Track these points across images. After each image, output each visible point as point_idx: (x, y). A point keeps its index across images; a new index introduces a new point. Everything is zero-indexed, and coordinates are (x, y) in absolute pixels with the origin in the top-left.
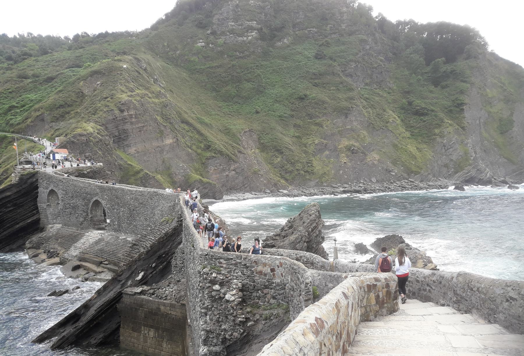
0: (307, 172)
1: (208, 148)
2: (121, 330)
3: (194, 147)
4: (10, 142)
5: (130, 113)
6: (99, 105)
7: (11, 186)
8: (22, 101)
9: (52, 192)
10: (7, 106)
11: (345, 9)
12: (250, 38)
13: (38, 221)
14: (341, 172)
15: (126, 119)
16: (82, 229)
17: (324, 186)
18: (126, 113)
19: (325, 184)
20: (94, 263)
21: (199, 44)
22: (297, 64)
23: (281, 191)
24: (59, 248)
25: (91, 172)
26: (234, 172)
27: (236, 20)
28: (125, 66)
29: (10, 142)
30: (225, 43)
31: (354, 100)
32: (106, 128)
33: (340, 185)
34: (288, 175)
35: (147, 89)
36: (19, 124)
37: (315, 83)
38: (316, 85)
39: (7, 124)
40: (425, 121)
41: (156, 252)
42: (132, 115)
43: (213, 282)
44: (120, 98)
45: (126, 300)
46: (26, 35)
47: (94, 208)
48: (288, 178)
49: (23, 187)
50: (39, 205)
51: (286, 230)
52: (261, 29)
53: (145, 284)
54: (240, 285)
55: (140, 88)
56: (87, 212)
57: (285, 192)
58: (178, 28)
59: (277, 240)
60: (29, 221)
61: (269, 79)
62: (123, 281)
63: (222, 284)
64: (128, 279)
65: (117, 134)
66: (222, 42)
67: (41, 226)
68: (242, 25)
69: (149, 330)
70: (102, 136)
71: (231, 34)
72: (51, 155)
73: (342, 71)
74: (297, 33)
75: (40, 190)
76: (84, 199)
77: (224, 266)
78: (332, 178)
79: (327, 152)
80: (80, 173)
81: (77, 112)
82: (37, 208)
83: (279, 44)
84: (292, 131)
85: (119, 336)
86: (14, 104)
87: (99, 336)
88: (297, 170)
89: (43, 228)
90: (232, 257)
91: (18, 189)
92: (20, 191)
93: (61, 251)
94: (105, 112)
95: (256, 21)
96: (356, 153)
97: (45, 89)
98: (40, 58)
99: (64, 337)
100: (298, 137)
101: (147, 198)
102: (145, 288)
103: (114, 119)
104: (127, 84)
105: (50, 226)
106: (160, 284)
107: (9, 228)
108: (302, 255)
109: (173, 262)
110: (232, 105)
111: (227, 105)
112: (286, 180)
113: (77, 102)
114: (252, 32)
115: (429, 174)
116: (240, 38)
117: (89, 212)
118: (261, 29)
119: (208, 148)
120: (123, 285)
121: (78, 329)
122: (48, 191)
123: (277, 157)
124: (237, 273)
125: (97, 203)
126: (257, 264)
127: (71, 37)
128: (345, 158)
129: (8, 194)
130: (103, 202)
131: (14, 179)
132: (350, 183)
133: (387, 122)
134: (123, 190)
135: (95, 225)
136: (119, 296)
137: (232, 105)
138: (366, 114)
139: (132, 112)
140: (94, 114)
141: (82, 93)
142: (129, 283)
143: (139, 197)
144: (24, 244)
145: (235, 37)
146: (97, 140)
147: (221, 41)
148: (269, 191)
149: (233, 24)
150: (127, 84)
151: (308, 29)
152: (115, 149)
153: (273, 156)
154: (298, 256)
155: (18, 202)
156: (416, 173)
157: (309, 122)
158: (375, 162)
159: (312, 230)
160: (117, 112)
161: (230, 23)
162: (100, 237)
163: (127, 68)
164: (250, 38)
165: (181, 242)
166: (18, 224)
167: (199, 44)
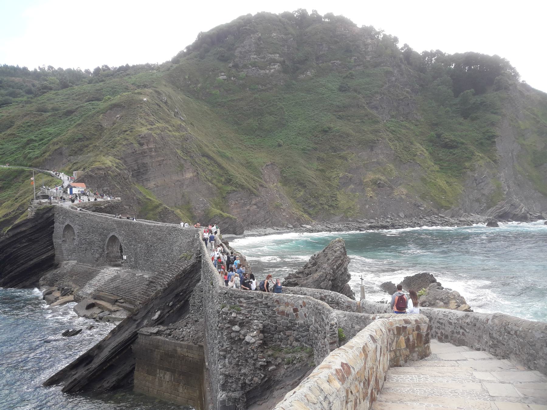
0: (331, 206)
1: (229, 181)
2: (136, 373)
3: (215, 181)
4: (27, 176)
5: (150, 147)
6: (118, 138)
7: (28, 221)
8: (41, 135)
9: (68, 227)
10: (25, 140)
11: (369, 41)
12: (272, 71)
13: (53, 257)
14: (367, 206)
15: (145, 153)
16: (98, 265)
17: (349, 221)
18: (145, 147)
19: (350, 219)
20: (109, 301)
21: (221, 77)
22: (321, 96)
23: (304, 226)
24: (74, 286)
25: (109, 206)
26: (255, 207)
27: (258, 53)
28: (145, 99)
29: (27, 176)
30: (247, 76)
31: (380, 132)
32: (125, 161)
33: (366, 220)
34: (311, 209)
35: (167, 122)
36: (37, 158)
37: (339, 115)
38: (340, 118)
39: (25, 158)
40: (454, 154)
41: (173, 290)
42: (151, 148)
43: (233, 322)
44: (139, 131)
45: (141, 340)
46: (46, 69)
47: (111, 244)
48: (312, 212)
49: (39, 221)
50: (54, 240)
51: (309, 268)
52: (284, 62)
53: (162, 323)
54: (261, 326)
55: (160, 121)
56: (103, 248)
57: (308, 227)
58: (200, 61)
59: (300, 277)
60: (43, 257)
61: (291, 111)
62: (139, 321)
63: (241, 325)
64: (144, 318)
65: (136, 168)
66: (244, 75)
67: (56, 262)
68: (264, 58)
69: (165, 374)
70: (121, 170)
71: (253, 67)
72: (69, 189)
73: (367, 104)
74: (320, 65)
75: (56, 225)
76: (100, 235)
77: (244, 305)
78: (357, 213)
79: (352, 186)
80: (97, 208)
81: (95, 146)
82: (52, 244)
83: (302, 76)
84: (316, 164)
85: (133, 380)
86: (33, 137)
87: (111, 380)
88: (321, 204)
89: (58, 265)
90: (252, 296)
91: (34, 224)
92: (36, 226)
93: (75, 288)
94: (124, 145)
95: (278, 53)
96: (382, 187)
97: (65, 122)
98: (60, 92)
99: (75, 380)
100: (322, 171)
101: (165, 233)
102: (162, 328)
103: (133, 153)
104: (147, 117)
105: (65, 262)
106: (177, 324)
107: (23, 264)
108: (327, 294)
109: (191, 301)
110: (254, 138)
111: (249, 138)
112: (310, 214)
113: (95, 135)
114: (274, 65)
115: (460, 209)
116: (262, 71)
117: (105, 248)
118: (284, 62)
119: (229, 181)
120: (138, 325)
121: (91, 372)
122: (64, 226)
123: (300, 191)
124: (258, 313)
125: (114, 239)
126: (279, 303)
127: (92, 70)
128: (371, 192)
129: (23, 229)
130: (120, 238)
131: (30, 213)
132: (376, 218)
133: (415, 156)
134: (141, 225)
135: (111, 261)
137: (254, 138)
138: (392, 147)
139: (152, 146)
140: (113, 148)
141: (101, 126)
142: (145, 322)
143: (157, 233)
144: (38, 281)
145: (258, 70)
146: (116, 174)
147: (243, 74)
148: (291, 226)
149: (255, 56)
150: (147, 117)
151: (332, 62)
152: (134, 183)
153: (296, 189)
154: (322, 295)
155: (33, 237)
156: (447, 208)
157: (333, 155)
158: (403, 196)
159: (338, 268)
160: (136, 145)
161: (252, 56)
162: (116, 274)
163: (148, 101)
164: (272, 71)
165: (200, 279)
166: (32, 260)
167: (221, 77)
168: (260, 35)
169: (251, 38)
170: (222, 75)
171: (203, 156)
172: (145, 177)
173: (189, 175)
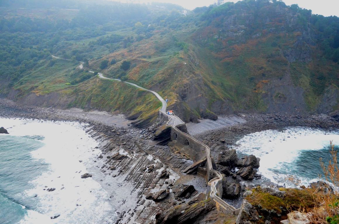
12: (240, 34)
13: (170, 138)
18: (186, 88)
27: (235, 24)
45: (198, 169)
68: (237, 27)
83: (254, 36)
95: (244, 25)
114: (241, 31)
115: (315, 112)
116: (235, 34)
119: (214, 97)
136: (198, 168)
139: (188, 87)
149: (233, 26)
160: (183, 88)
163: (186, 64)
168: (236, 15)
169: (232, 17)
171: (205, 85)
172: (185, 99)
173: (199, 95)
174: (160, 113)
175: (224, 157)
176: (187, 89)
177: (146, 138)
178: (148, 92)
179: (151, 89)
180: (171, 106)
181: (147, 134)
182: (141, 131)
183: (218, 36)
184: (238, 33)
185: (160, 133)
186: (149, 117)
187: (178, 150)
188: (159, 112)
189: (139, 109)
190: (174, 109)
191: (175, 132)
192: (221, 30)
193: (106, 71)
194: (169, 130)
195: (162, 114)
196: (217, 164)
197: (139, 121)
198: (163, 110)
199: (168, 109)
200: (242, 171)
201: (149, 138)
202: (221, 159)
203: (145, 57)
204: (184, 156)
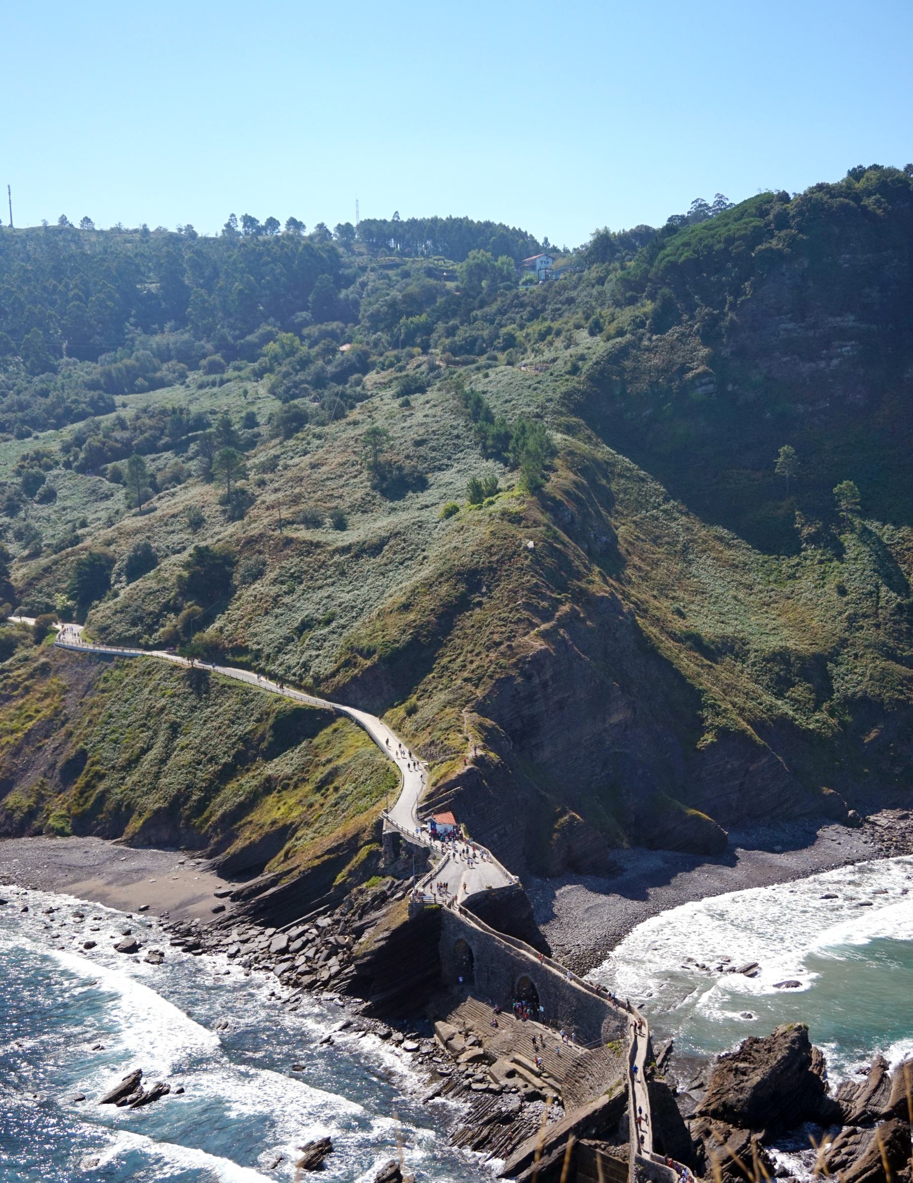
12: (835, 362)
18: (536, 681)
114: (841, 347)
149: (791, 326)
161: (784, 326)
168: (806, 265)
170: (702, 385)
173: (616, 719)
174: (387, 830)
175: (744, 1074)
176: (545, 685)
177: (306, 979)
178: (329, 717)
179: (341, 695)
180: (449, 786)
181: (311, 953)
182: (280, 941)
183: (711, 382)
184: (822, 359)
185: (377, 945)
186: (326, 857)
187: (479, 1044)
188: (379, 824)
189: (273, 812)
190: (467, 804)
191: (461, 936)
192: (728, 350)
193: (102, 610)
194: (428, 922)
195: (396, 837)
196: (724, 1113)
197: (274, 882)
198: (403, 816)
199: (430, 806)
200: (844, 1151)
201: (325, 975)
202: (731, 1080)
203: (313, 522)
204: (511, 1074)
